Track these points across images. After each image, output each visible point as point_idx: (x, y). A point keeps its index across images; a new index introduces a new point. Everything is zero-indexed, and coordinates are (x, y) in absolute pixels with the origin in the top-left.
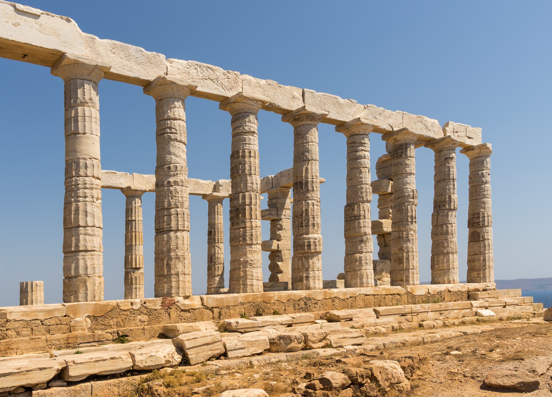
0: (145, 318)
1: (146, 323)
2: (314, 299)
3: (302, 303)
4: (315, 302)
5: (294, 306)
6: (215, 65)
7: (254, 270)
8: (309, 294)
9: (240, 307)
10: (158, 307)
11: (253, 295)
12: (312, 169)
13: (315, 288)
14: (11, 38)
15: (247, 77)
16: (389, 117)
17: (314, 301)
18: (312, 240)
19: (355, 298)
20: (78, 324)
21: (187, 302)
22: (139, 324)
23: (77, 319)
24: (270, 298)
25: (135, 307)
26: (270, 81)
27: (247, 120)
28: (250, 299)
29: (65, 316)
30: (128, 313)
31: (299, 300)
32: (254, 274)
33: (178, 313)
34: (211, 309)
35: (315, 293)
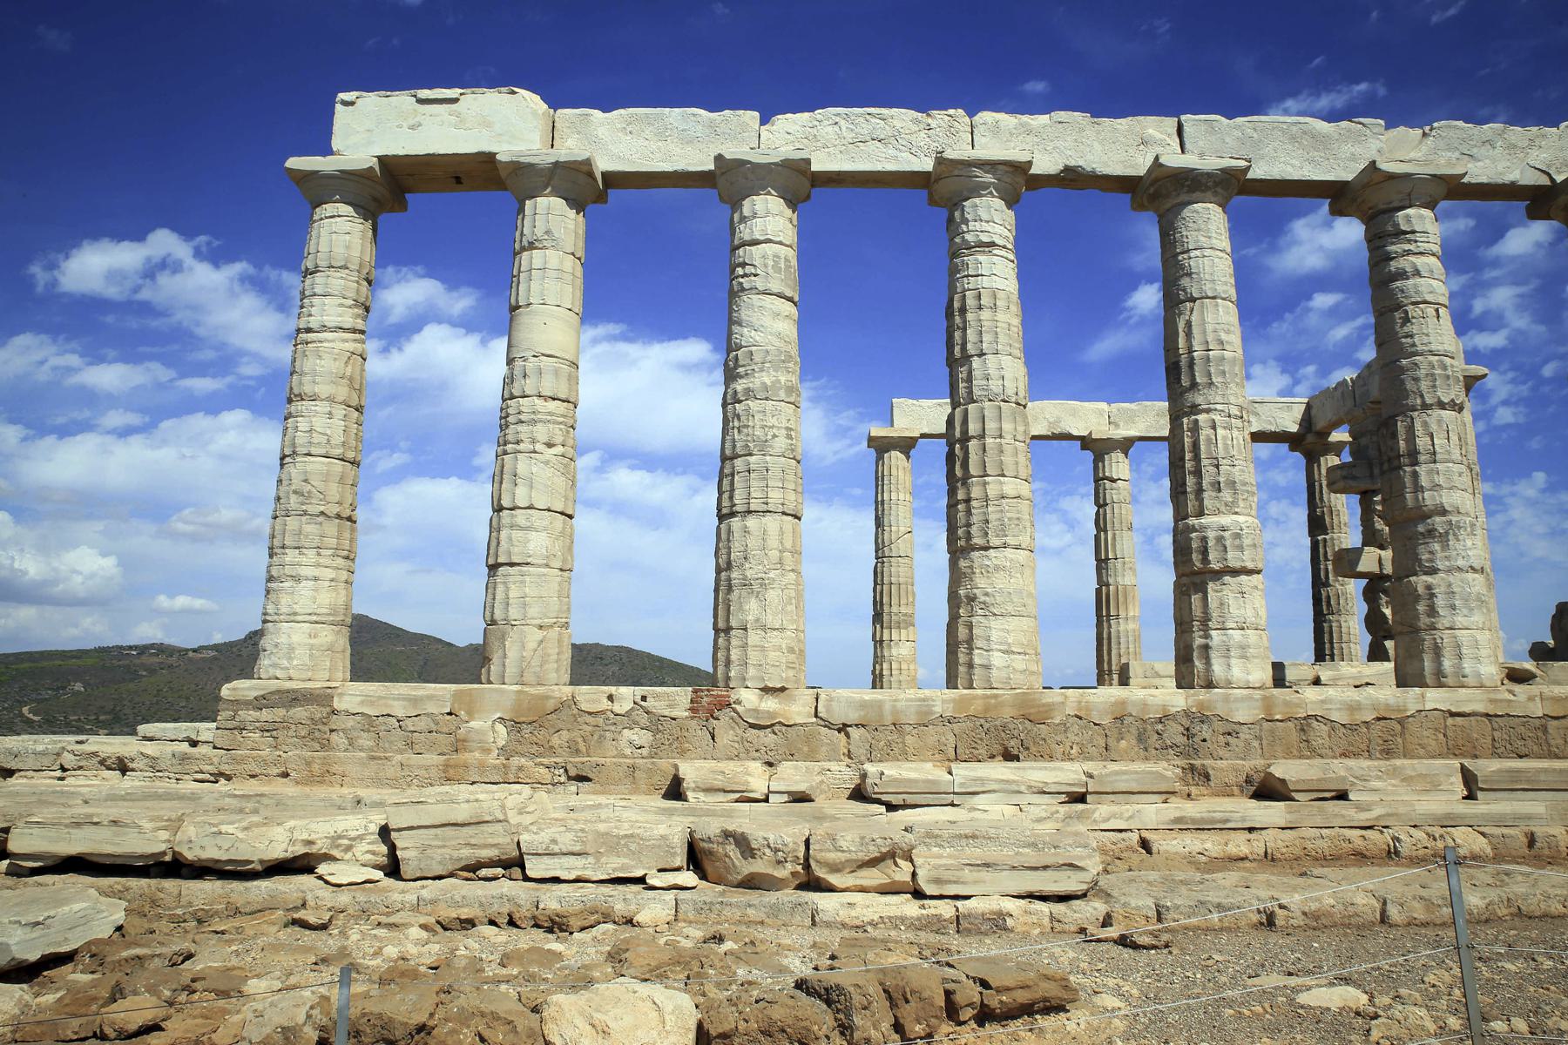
0: (642, 737)
1: (645, 752)
3: (1174, 733)
4: (1229, 728)
5: (1141, 738)
7: (995, 624)
8: (1201, 705)
10: (682, 713)
11: (986, 697)
12: (1203, 322)
14: (402, 152)
15: (986, 117)
16: (1530, 147)
17: (1220, 727)
18: (1211, 535)
19: (1401, 722)
20: (473, 736)
21: (770, 704)
22: (628, 751)
23: (472, 724)
24: (1050, 708)
25: (617, 708)
29: (450, 714)
30: (600, 721)
31: (1160, 721)
33: (740, 732)
34: (843, 728)
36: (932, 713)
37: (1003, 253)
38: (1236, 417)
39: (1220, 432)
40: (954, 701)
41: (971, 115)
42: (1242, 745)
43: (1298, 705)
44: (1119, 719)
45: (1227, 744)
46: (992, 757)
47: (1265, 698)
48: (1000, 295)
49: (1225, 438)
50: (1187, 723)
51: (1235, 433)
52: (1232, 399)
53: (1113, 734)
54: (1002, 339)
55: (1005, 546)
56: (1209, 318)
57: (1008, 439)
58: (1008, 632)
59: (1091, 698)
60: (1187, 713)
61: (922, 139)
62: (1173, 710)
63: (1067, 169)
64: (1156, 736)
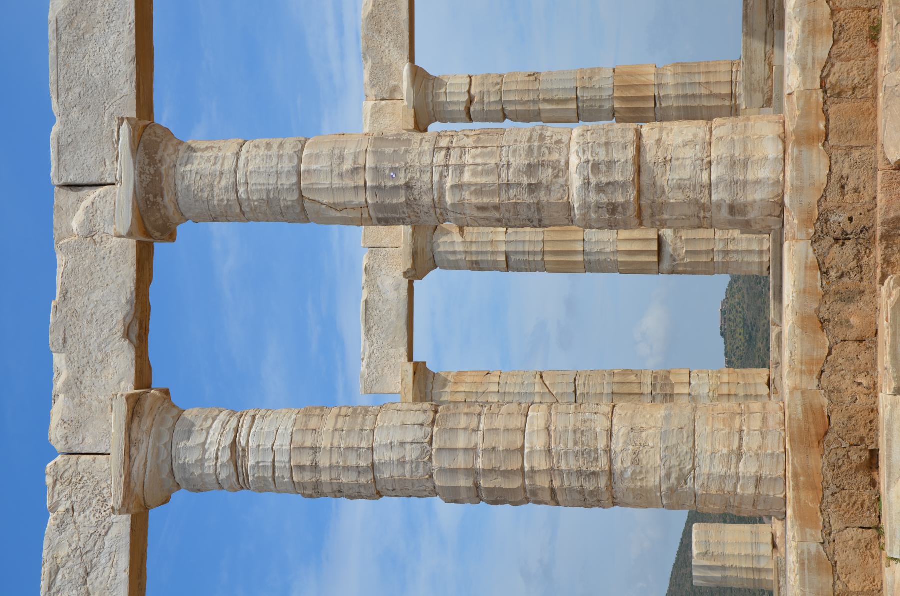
2: (824, 197)
4: (835, 188)
5: (848, 298)
6: (39, 563)
7: (704, 469)
9: (839, 547)
11: (797, 487)
12: (331, 190)
13: (780, 184)
15: (56, 434)
17: (834, 197)
18: (593, 198)
24: (809, 409)
26: (55, 338)
27: (197, 472)
28: (811, 501)
31: (825, 273)
32: (719, 469)
35: (798, 190)
36: (818, 552)
37: (244, 432)
38: (448, 156)
39: (467, 178)
40: (802, 528)
41: (54, 454)
42: (857, 172)
43: (808, 100)
44: (823, 322)
45: (856, 190)
46: (874, 484)
47: (798, 143)
48: (298, 439)
49: (475, 174)
50: (829, 241)
51: (468, 159)
52: (427, 160)
53: (840, 333)
54: (354, 442)
55: (608, 451)
56: (325, 182)
57: (477, 439)
58: (714, 453)
59: (797, 358)
60: (815, 240)
61: (86, 520)
62: (812, 257)
63: (127, 335)
64: (846, 280)
